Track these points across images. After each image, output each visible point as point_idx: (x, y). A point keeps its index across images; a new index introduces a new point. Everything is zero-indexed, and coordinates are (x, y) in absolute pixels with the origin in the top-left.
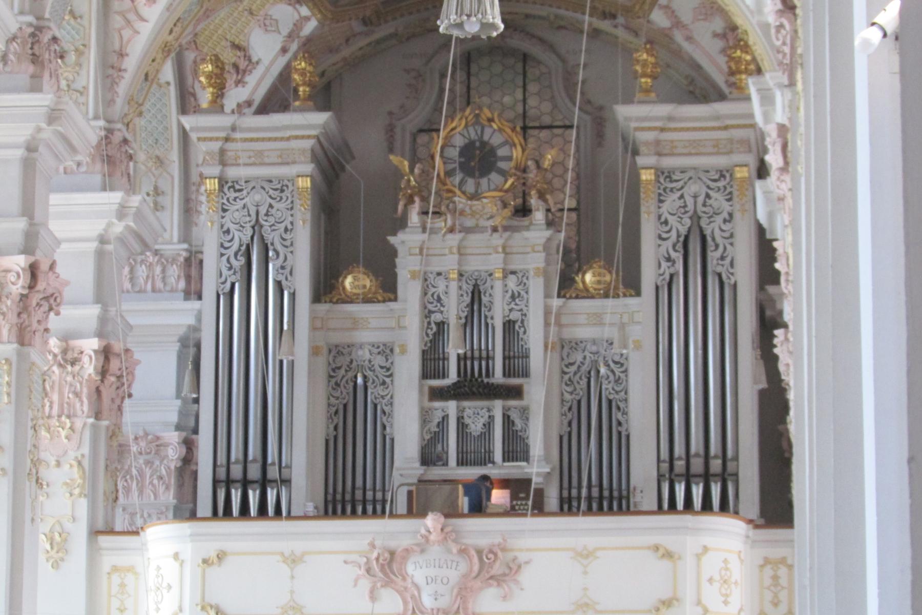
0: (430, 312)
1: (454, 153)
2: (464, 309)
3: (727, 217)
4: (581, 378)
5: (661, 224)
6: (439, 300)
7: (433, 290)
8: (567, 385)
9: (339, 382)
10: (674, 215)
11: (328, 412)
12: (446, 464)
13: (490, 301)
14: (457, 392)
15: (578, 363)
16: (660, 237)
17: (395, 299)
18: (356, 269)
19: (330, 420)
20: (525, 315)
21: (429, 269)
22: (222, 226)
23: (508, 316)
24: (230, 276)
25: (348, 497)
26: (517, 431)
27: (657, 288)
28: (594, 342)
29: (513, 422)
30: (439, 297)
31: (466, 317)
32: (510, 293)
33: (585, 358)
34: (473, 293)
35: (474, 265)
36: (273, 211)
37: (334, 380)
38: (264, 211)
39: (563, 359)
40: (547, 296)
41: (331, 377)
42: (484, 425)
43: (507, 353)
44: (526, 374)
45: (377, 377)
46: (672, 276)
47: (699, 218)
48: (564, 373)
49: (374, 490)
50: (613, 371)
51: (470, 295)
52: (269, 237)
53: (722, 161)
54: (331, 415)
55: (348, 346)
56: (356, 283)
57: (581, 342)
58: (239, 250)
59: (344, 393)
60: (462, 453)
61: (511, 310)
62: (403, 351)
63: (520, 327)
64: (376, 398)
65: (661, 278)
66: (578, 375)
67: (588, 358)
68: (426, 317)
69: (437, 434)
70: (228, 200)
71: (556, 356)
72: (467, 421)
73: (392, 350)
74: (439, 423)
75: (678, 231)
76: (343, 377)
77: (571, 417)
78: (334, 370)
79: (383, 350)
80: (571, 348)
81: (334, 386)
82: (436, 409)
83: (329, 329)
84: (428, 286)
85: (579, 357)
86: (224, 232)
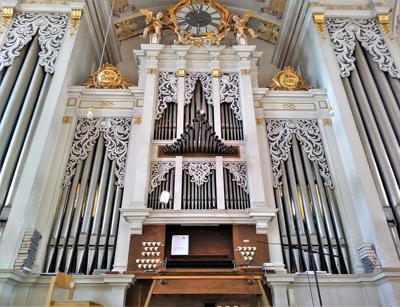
0: (162, 95)
1: (183, 15)
2: (189, 94)
3: (380, 42)
6: (170, 88)
7: (168, 82)
9: (81, 144)
10: (343, 39)
11: (68, 166)
13: (210, 91)
14: (182, 150)
16: (335, 50)
17: (137, 86)
18: (107, 68)
19: (68, 173)
20: (238, 99)
21: (162, 69)
22: (9, 35)
23: (224, 100)
24: (4, 62)
25: (72, 242)
26: (236, 182)
28: (291, 121)
29: (232, 174)
30: (170, 86)
31: (191, 100)
32: (225, 86)
33: (286, 131)
34: (196, 85)
35: (199, 68)
36: (50, 29)
37: (77, 143)
38: (44, 28)
39: (268, 132)
40: (253, 86)
42: (206, 177)
43: (223, 124)
44: (241, 137)
45: (115, 140)
46: (351, 72)
49: (99, 236)
50: (309, 141)
51: (194, 86)
52: (42, 39)
53: (367, 14)
54: (69, 169)
55: (94, 119)
56: (107, 76)
57: (281, 121)
58: (18, 48)
59: (84, 151)
60: (187, 200)
61: (226, 96)
62: (139, 121)
63: (233, 107)
64: (111, 156)
66: (283, 142)
67: (288, 131)
68: (159, 98)
69: (164, 183)
70: (19, 22)
71: (263, 127)
72: (191, 173)
73: (130, 123)
74: (166, 174)
76: (86, 140)
78: (79, 135)
79: (122, 122)
80: (273, 125)
81: (77, 147)
82: (164, 164)
83: (80, 108)
84: (161, 80)
85: (282, 132)
86: (9, 38)
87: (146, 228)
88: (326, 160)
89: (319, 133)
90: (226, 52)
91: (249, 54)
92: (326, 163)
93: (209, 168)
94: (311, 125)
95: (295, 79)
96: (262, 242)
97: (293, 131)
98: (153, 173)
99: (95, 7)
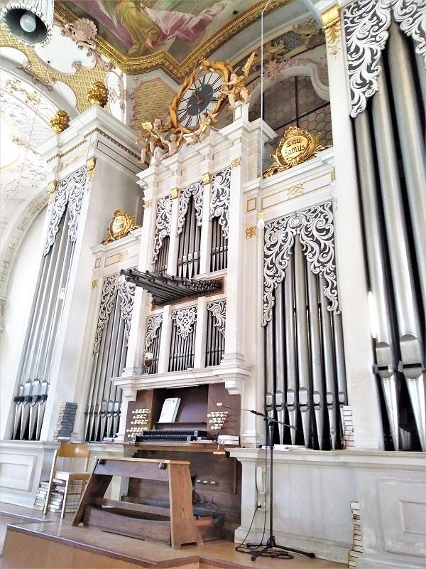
0: (159, 230)
4: (282, 259)
5: (350, 54)
7: (162, 211)
8: (269, 269)
12: (154, 371)
15: (280, 242)
20: (227, 208)
27: (353, 120)
28: (296, 215)
30: (165, 216)
35: (191, 179)
39: (265, 243)
41: (102, 303)
45: (127, 296)
46: (370, 101)
47: (399, 24)
48: (267, 256)
50: (318, 242)
61: (215, 208)
63: (222, 221)
65: (356, 107)
67: (290, 234)
72: (179, 323)
75: (372, 50)
77: (273, 303)
80: (273, 230)
87: (141, 394)
88: (335, 268)
89: (332, 223)
90: (218, 141)
91: (241, 131)
92: (335, 274)
93: (194, 313)
94: (322, 213)
95: (299, 145)
96: (233, 405)
97: (296, 230)
98: (148, 330)
99: (112, 140)
